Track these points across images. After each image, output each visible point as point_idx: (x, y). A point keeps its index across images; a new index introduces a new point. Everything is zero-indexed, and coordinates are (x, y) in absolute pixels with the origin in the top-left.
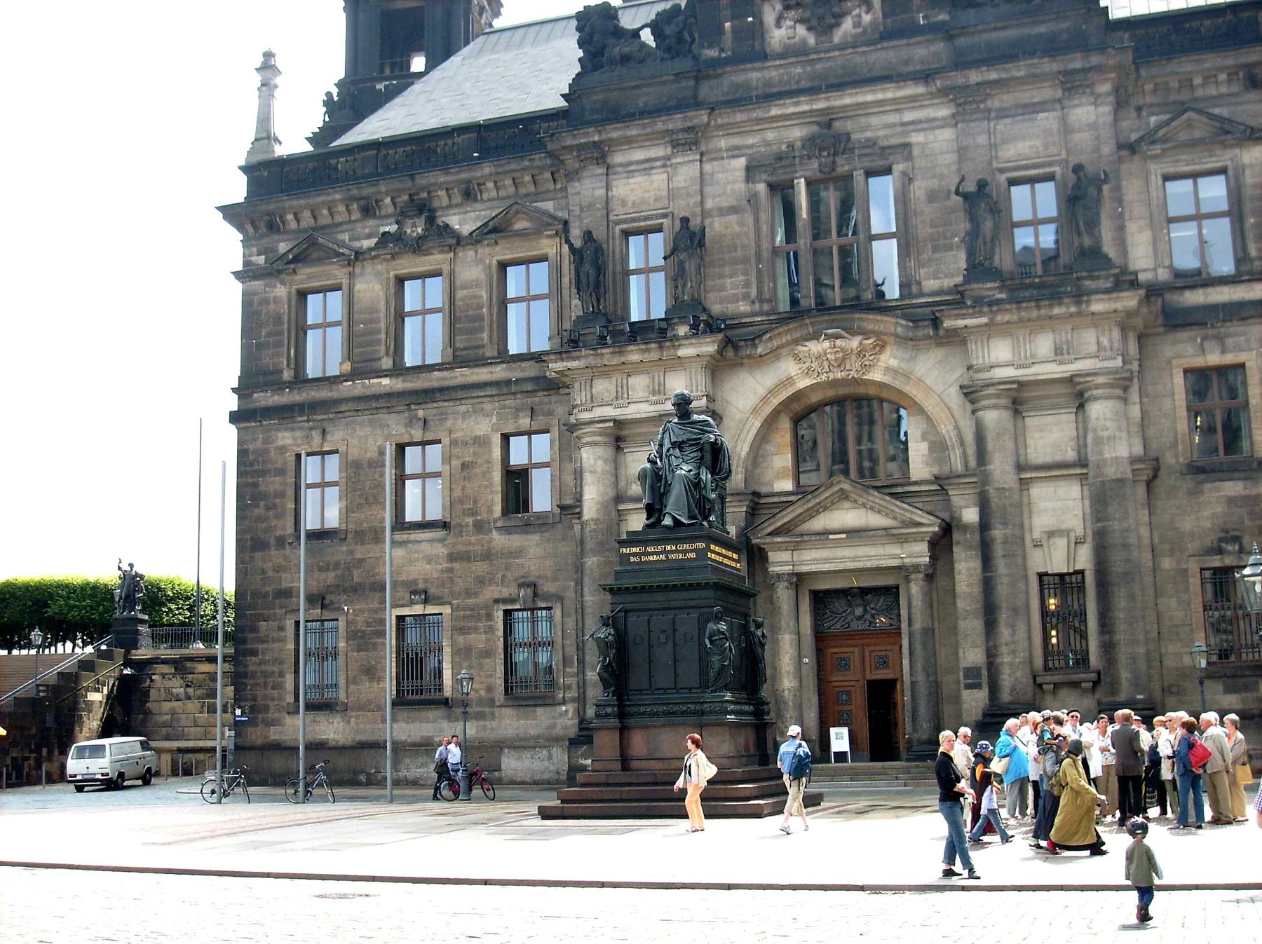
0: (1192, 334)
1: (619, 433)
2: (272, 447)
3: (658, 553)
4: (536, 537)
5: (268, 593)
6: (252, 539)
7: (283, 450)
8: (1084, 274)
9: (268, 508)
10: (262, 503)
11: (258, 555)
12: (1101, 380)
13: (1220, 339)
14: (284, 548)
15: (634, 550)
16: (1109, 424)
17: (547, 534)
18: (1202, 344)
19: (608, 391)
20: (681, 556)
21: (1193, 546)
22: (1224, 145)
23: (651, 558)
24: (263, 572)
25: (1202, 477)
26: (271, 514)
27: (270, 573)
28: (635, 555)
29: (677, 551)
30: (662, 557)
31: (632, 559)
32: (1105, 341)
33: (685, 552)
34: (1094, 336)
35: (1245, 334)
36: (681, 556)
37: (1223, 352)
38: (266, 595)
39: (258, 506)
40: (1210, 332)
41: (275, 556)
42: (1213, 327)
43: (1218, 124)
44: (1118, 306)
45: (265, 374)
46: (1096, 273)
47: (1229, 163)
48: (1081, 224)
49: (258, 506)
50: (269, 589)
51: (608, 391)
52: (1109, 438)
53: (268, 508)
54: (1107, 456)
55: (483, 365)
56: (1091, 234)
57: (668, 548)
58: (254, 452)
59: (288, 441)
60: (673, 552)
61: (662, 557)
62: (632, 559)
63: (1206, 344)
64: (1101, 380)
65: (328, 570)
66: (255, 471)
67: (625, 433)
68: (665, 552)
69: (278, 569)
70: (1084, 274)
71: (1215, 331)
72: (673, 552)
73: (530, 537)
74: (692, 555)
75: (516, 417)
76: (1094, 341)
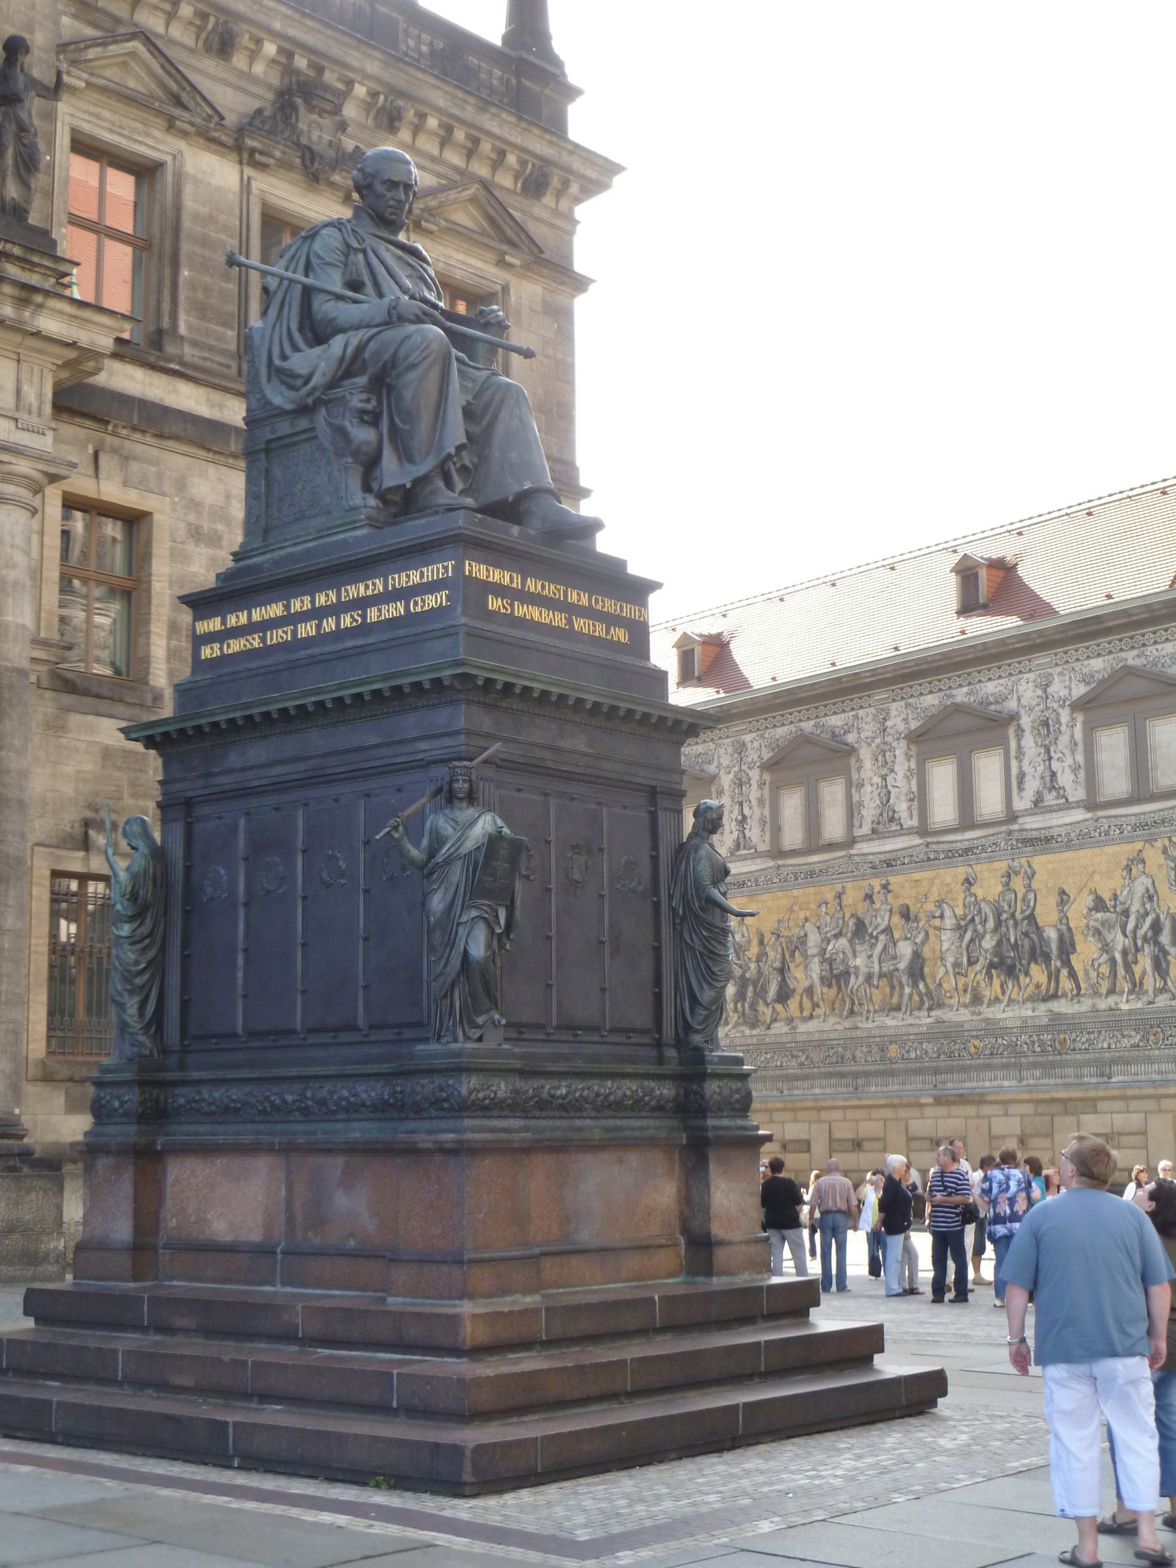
0: (83, 433)
8: (17, 251)
12: (23, 466)
13: (127, 459)
15: (497, 576)
16: (19, 558)
18: (96, 455)
20: (600, 630)
21: (41, 827)
22: (171, 126)
23: (534, 613)
25: (68, 699)
28: (500, 590)
29: (589, 613)
30: (558, 619)
31: (494, 604)
32: (30, 393)
34: (13, 376)
35: (157, 463)
36: (600, 630)
37: (125, 484)
40: (109, 440)
42: (114, 434)
43: (174, 87)
44: (84, 337)
46: (36, 259)
47: (169, 159)
48: (10, 153)
52: (16, 583)
54: (9, 618)
56: (25, 184)
57: (573, 596)
61: (558, 619)
62: (494, 604)
63: (104, 459)
64: (23, 466)
70: (17, 251)
71: (117, 441)
76: (10, 386)
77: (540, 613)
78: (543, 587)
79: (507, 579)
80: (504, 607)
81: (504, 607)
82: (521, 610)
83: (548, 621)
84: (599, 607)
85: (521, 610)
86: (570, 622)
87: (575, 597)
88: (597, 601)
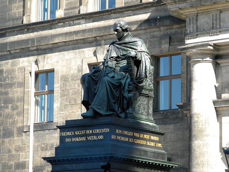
1: (216, 53)
2: (16, 68)
3: (81, 136)
4: (171, 127)
5: (12, 165)
6: (4, 130)
7: (23, 69)
9: (13, 109)
10: (10, 105)
11: (7, 140)
14: (22, 135)
17: (178, 125)
19: (207, 23)
20: (95, 138)
24: (10, 151)
26: (15, 112)
27: (14, 152)
29: (93, 134)
30: (84, 139)
31: (67, 140)
33: (97, 135)
36: (95, 138)
38: (10, 167)
39: (7, 107)
41: (17, 141)
45: (13, 20)
49: (7, 107)
50: (12, 163)
51: (207, 23)
53: (13, 109)
55: (141, 9)
58: (7, 71)
59: (26, 64)
60: (90, 135)
61: (84, 139)
62: (67, 140)
65: (46, 149)
66: (6, 84)
67: (221, 52)
68: (86, 135)
69: (19, 149)
72: (90, 135)
73: (168, 126)
74: (101, 137)
75: (160, 44)
77: (79, 139)
78: (80, 132)
79: (70, 133)
80: (69, 140)
81: (69, 140)
82: (74, 139)
83: (81, 140)
84: (95, 132)
85: (74, 139)
86: (86, 138)
87: (88, 132)
88: (94, 131)
